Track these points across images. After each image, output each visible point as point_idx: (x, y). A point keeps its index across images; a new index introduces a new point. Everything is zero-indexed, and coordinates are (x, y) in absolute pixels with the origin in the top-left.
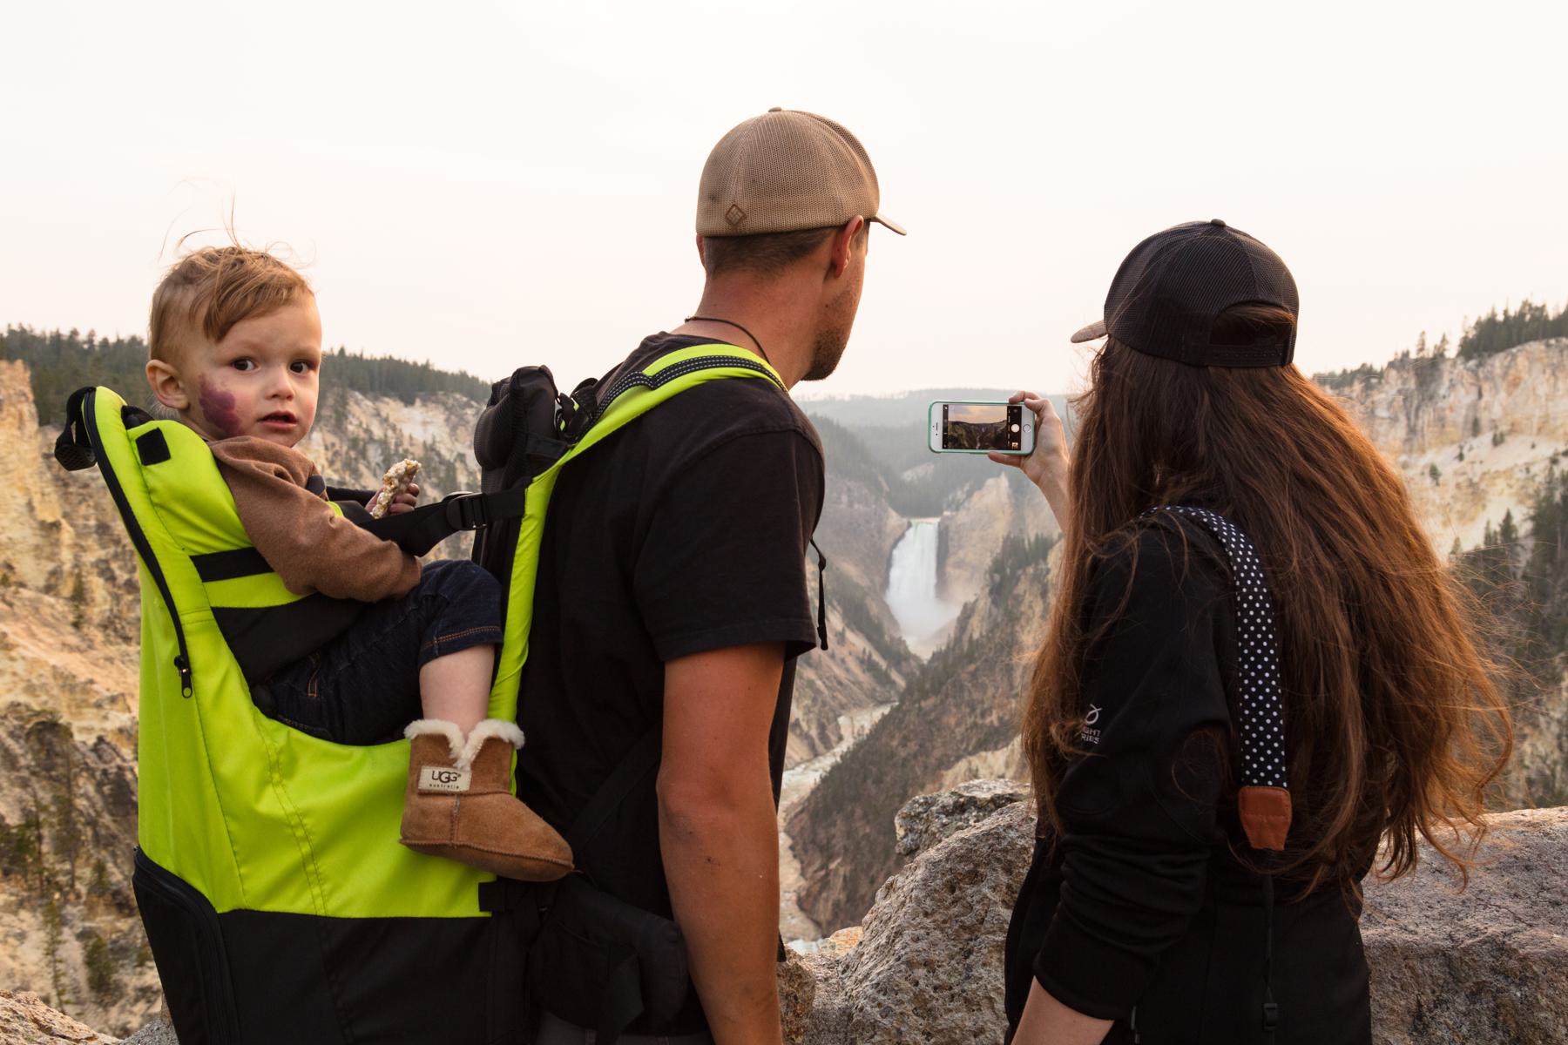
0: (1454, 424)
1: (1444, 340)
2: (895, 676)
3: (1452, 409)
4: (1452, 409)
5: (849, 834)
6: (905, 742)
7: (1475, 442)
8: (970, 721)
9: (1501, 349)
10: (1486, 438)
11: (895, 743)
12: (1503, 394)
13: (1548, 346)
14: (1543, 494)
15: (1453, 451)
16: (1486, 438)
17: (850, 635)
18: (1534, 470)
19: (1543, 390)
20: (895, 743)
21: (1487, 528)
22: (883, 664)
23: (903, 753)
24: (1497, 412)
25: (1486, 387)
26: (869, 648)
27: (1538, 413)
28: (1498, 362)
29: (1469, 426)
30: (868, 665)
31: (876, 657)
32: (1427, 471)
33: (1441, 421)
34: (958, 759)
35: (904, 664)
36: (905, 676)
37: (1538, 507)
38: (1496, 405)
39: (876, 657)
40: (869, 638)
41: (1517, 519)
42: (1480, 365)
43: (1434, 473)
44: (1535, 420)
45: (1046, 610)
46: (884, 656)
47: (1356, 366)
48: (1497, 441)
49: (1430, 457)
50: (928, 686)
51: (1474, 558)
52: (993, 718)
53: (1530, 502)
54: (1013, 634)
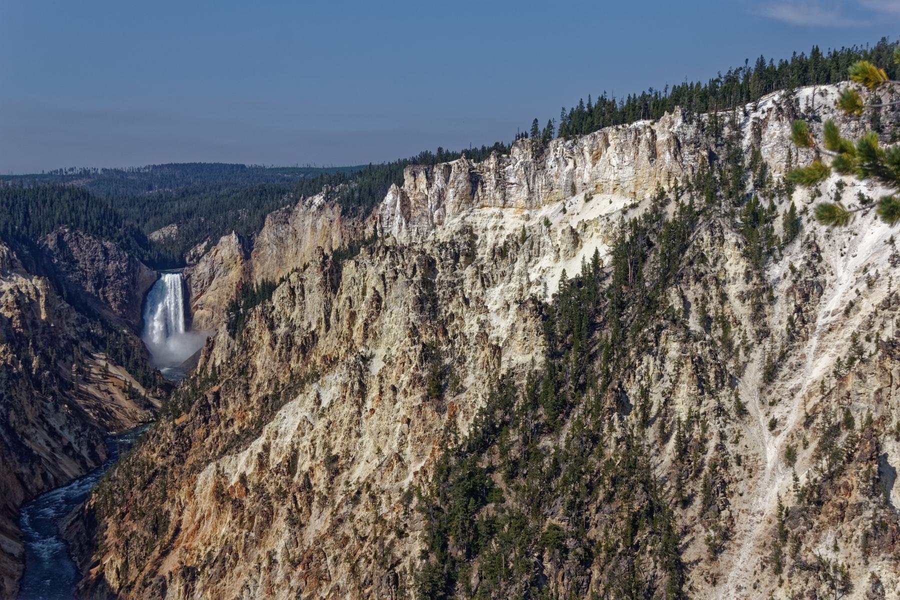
0: (559, 187)
1: (550, 126)
3: (557, 176)
4: (557, 176)
5: (118, 533)
6: (165, 454)
7: (573, 200)
8: (216, 431)
9: (588, 132)
10: (580, 197)
11: (155, 455)
12: (589, 165)
13: (618, 130)
14: (618, 236)
15: (558, 206)
16: (580, 197)
17: (112, 369)
18: (612, 218)
19: (615, 161)
20: (155, 455)
21: (583, 262)
22: (142, 392)
23: (160, 462)
24: (586, 178)
25: (578, 160)
27: (612, 177)
28: (586, 142)
29: (569, 188)
31: (136, 386)
32: (542, 221)
33: (550, 186)
34: (208, 462)
37: (615, 244)
38: (586, 171)
39: (136, 386)
41: (602, 253)
42: (574, 144)
43: (547, 223)
44: (611, 183)
45: (274, 339)
47: (492, 145)
48: (588, 199)
49: (546, 211)
50: (180, 406)
51: (578, 283)
52: (235, 428)
53: (610, 242)
54: (248, 359)
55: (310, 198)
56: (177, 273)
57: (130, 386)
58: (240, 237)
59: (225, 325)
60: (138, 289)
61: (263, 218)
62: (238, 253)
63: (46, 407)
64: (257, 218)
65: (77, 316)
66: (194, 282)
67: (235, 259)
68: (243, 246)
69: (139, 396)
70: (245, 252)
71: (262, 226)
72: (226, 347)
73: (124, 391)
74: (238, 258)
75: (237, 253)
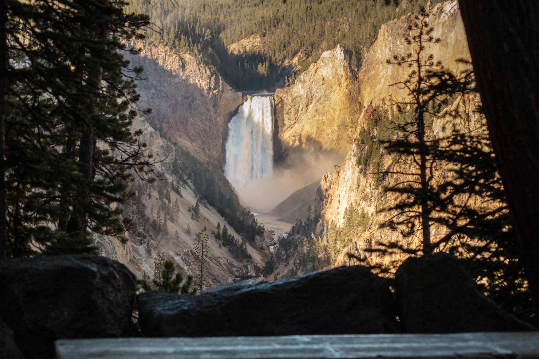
2: (250, 250)
17: (203, 211)
22: (238, 239)
26: (223, 223)
30: (225, 240)
31: (231, 232)
35: (258, 238)
36: (261, 250)
39: (231, 232)
40: (222, 213)
46: (238, 231)
55: (439, 5)
56: (266, 96)
57: (225, 230)
58: (347, 52)
59: (354, 160)
60: (220, 114)
61: (376, 29)
62: (343, 73)
63: (136, 250)
64: (367, 29)
65: (162, 144)
66: (286, 107)
67: (339, 79)
68: (350, 64)
69: (236, 245)
70: (352, 71)
71: (373, 39)
72: (355, 186)
73: (217, 237)
74: (344, 78)
75: (341, 71)
